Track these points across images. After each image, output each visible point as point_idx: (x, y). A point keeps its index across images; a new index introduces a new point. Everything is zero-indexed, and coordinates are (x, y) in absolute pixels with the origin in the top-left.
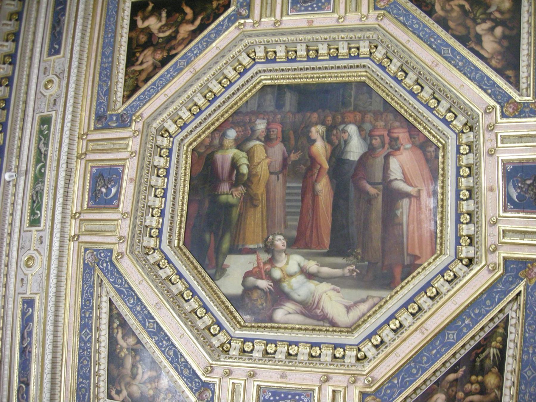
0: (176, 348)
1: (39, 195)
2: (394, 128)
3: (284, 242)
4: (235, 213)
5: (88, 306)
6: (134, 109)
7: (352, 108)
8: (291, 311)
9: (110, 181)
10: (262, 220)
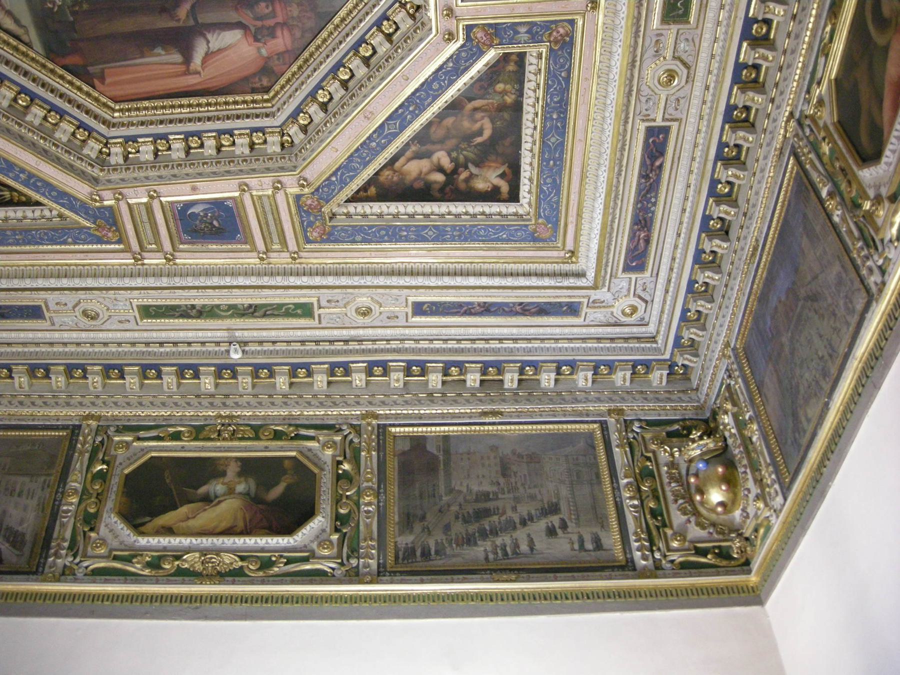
2: (290, 31)
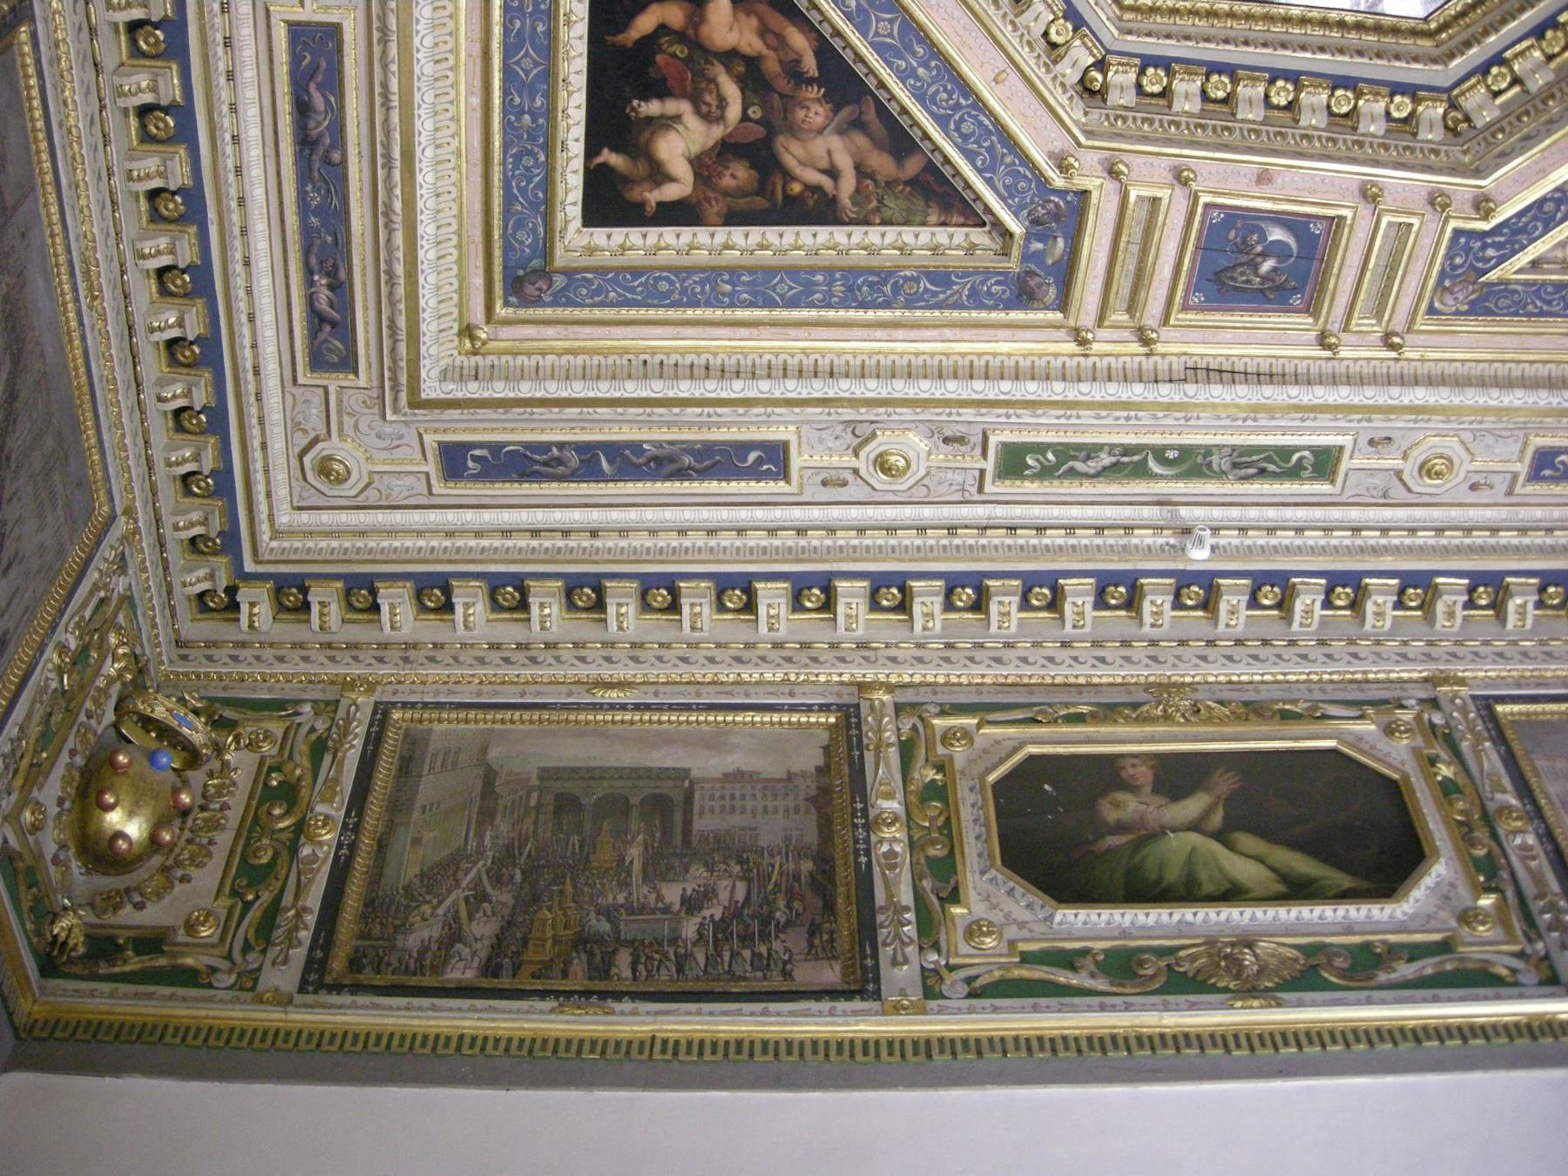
9: (1243, 247)
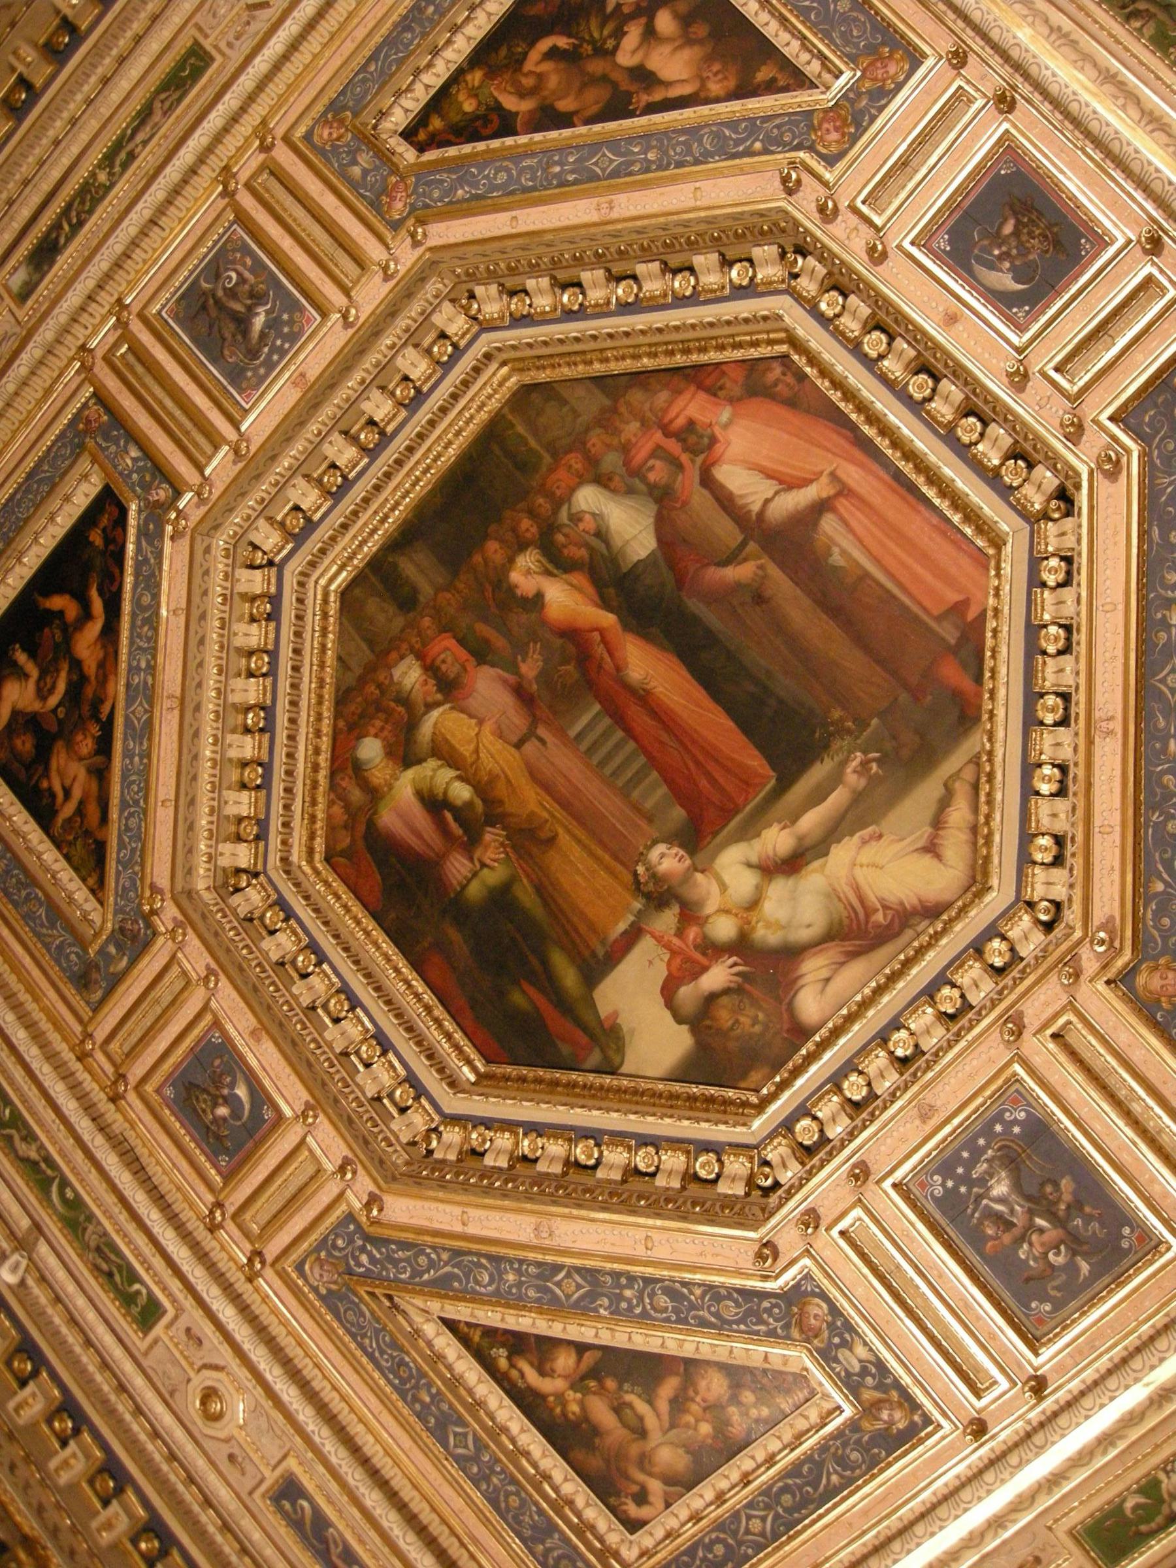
0: (661, 1280)
1: (106, 1250)
2: (665, 410)
3: (675, 850)
4: (526, 895)
5: (411, 1376)
6: (132, 894)
7: (547, 459)
8: (824, 973)
9: (217, 1081)
10: (591, 854)
